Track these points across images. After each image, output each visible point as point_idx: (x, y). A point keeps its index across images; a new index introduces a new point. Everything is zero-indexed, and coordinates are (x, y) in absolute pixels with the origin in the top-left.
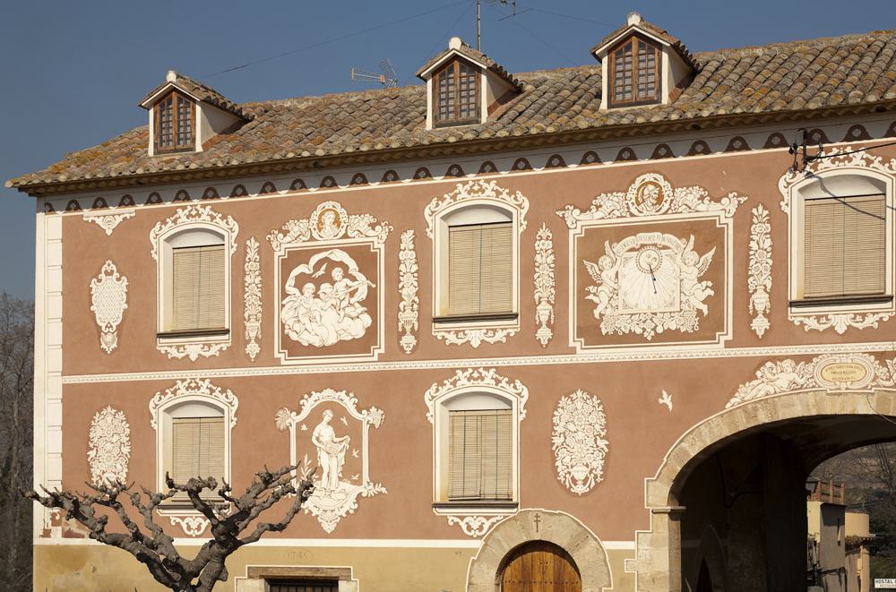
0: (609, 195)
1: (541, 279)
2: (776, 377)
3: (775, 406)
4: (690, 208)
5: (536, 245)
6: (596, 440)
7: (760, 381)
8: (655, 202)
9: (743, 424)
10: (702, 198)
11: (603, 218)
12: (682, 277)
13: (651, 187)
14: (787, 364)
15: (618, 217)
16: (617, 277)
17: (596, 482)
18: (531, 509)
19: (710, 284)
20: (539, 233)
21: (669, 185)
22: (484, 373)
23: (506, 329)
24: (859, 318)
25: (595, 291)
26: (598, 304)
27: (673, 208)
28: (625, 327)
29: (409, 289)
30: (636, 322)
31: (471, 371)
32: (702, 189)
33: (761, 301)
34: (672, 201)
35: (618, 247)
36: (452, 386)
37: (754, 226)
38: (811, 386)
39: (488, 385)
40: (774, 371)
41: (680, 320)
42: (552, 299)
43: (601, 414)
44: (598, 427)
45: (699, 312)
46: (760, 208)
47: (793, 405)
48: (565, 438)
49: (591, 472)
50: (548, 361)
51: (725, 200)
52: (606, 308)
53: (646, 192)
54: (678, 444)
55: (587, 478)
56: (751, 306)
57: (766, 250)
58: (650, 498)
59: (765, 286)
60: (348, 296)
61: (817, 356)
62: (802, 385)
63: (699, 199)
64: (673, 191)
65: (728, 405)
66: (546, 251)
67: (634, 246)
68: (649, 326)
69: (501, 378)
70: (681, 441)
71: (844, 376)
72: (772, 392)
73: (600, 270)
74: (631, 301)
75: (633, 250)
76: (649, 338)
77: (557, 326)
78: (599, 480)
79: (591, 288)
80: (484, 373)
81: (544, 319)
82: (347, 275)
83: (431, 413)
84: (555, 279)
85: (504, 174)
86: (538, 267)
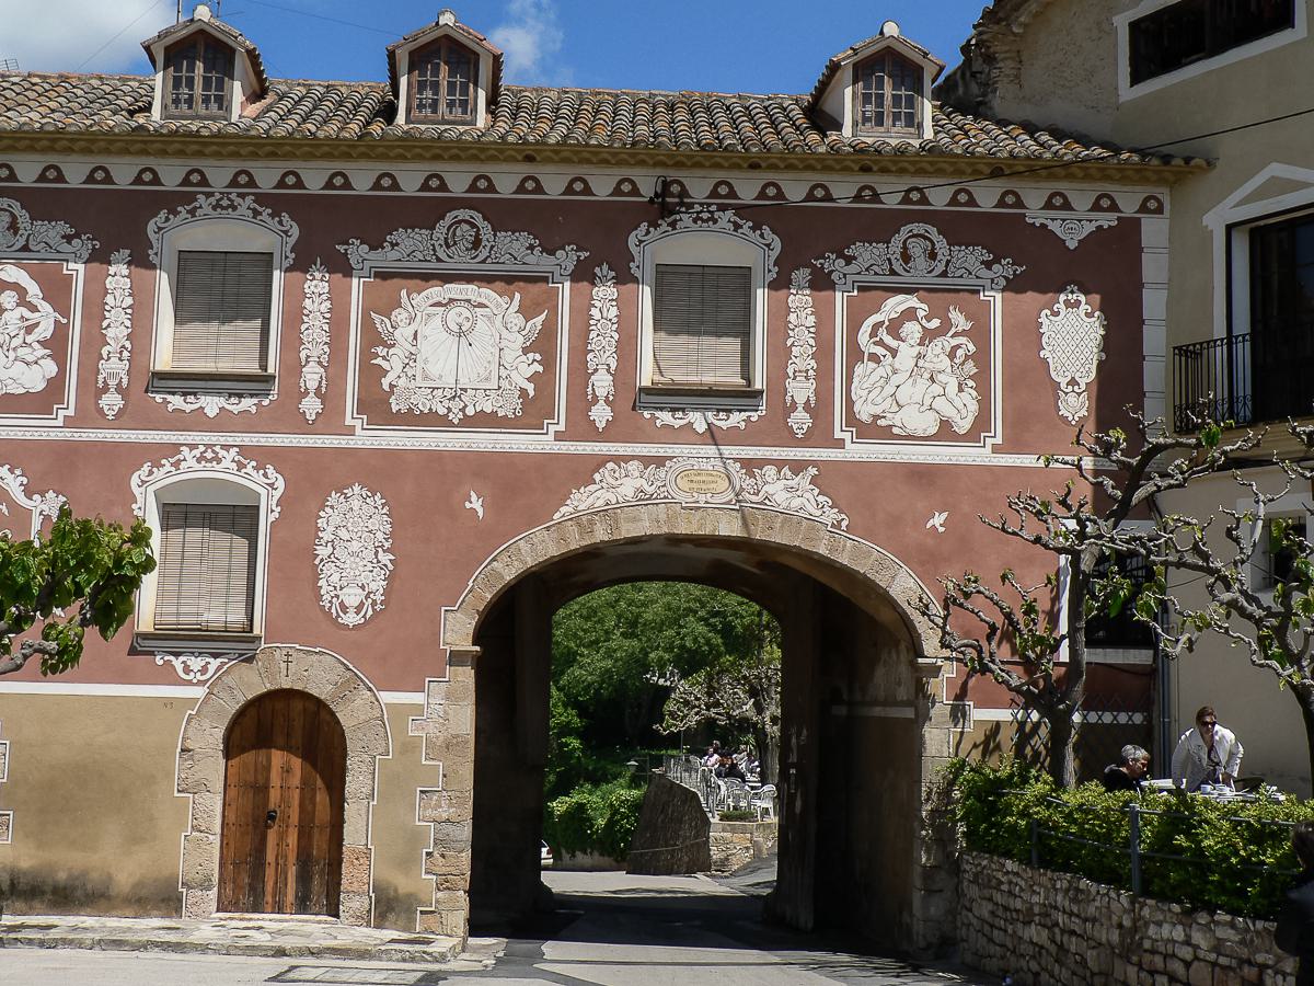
0: (409, 231)
2: (619, 482)
3: (616, 521)
4: (516, 259)
5: (306, 286)
6: (376, 553)
9: (576, 542)
10: (531, 248)
12: (502, 346)
13: (466, 227)
14: (634, 466)
15: (420, 260)
16: (415, 338)
17: (374, 610)
19: (538, 357)
22: (222, 453)
27: (493, 256)
29: (117, 329)
30: (438, 400)
31: (202, 448)
33: (602, 383)
34: (492, 247)
35: (418, 299)
36: (173, 469)
38: (662, 496)
39: (226, 469)
40: (617, 475)
44: (380, 536)
46: (605, 267)
48: (334, 549)
49: (367, 597)
50: (291, 442)
53: (458, 232)
54: (489, 564)
55: (362, 604)
57: (610, 320)
60: (23, 332)
61: (671, 458)
63: (527, 249)
64: (495, 235)
68: (456, 405)
69: (246, 462)
70: (494, 560)
71: (704, 487)
72: (614, 501)
73: (392, 327)
74: (433, 370)
75: (438, 304)
76: (456, 421)
77: (330, 395)
78: (378, 607)
79: (379, 349)
80: (222, 453)
81: (312, 385)
82: (23, 301)
83: (140, 502)
86: (308, 316)
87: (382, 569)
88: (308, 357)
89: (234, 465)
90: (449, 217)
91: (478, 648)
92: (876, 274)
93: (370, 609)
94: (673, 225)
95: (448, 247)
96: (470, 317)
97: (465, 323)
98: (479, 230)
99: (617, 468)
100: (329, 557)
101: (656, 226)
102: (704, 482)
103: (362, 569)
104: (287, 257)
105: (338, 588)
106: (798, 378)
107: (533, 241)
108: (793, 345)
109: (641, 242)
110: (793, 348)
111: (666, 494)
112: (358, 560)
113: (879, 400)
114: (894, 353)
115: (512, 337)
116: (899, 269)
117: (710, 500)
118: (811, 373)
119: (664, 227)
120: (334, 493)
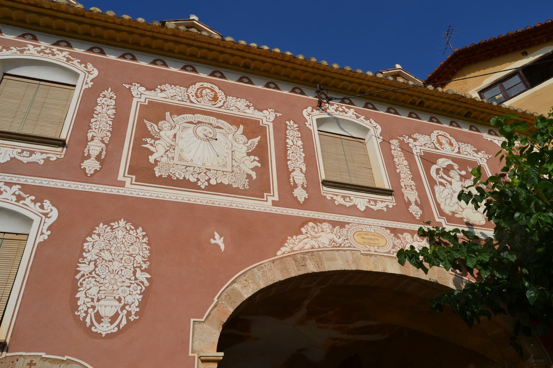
0: (173, 86)
1: (98, 123)
2: (318, 235)
3: (320, 259)
4: (239, 109)
5: (99, 99)
6: (135, 273)
7: (305, 236)
11: (166, 98)
12: (233, 149)
13: (208, 91)
14: (326, 226)
15: (179, 100)
17: (128, 320)
18: (24, 354)
19: (257, 158)
20: (104, 93)
21: (223, 93)
23: (46, 153)
24: (372, 203)
26: (154, 153)
27: (225, 106)
28: (180, 174)
30: (190, 173)
32: (248, 102)
33: (299, 177)
34: (225, 102)
35: (176, 118)
37: (288, 131)
38: (347, 245)
40: (316, 230)
43: (145, 246)
44: (139, 259)
45: (249, 176)
46: (292, 122)
47: (336, 260)
48: (96, 267)
49: (123, 308)
51: (265, 111)
52: (162, 157)
53: (204, 92)
54: (230, 285)
55: (117, 315)
56: (291, 180)
57: (299, 146)
58: (196, 343)
61: (348, 223)
62: (341, 244)
63: (246, 106)
64: (226, 97)
65: (279, 253)
66: (108, 106)
67: (193, 121)
68: (203, 178)
69: (25, 196)
70: (234, 282)
71: (372, 242)
72: (317, 246)
73: (159, 129)
74: (187, 156)
76: (203, 187)
78: (132, 318)
79: (148, 140)
85: (77, 50)
86: (97, 114)
87: (138, 285)
88: (95, 137)
89: (14, 198)
90: (198, 85)
91: (222, 354)
92: (429, 147)
93: (124, 318)
95: (197, 97)
98: (216, 93)
99: (316, 226)
100: (91, 273)
102: (371, 239)
103: (119, 284)
104: (87, 83)
105: (95, 300)
106: (408, 189)
107: (249, 104)
108: (400, 172)
109: (309, 114)
110: (401, 174)
111: (350, 245)
112: (117, 277)
113: (451, 204)
114: (451, 183)
116: (439, 148)
117: (377, 250)
118: (413, 187)
120: (101, 224)
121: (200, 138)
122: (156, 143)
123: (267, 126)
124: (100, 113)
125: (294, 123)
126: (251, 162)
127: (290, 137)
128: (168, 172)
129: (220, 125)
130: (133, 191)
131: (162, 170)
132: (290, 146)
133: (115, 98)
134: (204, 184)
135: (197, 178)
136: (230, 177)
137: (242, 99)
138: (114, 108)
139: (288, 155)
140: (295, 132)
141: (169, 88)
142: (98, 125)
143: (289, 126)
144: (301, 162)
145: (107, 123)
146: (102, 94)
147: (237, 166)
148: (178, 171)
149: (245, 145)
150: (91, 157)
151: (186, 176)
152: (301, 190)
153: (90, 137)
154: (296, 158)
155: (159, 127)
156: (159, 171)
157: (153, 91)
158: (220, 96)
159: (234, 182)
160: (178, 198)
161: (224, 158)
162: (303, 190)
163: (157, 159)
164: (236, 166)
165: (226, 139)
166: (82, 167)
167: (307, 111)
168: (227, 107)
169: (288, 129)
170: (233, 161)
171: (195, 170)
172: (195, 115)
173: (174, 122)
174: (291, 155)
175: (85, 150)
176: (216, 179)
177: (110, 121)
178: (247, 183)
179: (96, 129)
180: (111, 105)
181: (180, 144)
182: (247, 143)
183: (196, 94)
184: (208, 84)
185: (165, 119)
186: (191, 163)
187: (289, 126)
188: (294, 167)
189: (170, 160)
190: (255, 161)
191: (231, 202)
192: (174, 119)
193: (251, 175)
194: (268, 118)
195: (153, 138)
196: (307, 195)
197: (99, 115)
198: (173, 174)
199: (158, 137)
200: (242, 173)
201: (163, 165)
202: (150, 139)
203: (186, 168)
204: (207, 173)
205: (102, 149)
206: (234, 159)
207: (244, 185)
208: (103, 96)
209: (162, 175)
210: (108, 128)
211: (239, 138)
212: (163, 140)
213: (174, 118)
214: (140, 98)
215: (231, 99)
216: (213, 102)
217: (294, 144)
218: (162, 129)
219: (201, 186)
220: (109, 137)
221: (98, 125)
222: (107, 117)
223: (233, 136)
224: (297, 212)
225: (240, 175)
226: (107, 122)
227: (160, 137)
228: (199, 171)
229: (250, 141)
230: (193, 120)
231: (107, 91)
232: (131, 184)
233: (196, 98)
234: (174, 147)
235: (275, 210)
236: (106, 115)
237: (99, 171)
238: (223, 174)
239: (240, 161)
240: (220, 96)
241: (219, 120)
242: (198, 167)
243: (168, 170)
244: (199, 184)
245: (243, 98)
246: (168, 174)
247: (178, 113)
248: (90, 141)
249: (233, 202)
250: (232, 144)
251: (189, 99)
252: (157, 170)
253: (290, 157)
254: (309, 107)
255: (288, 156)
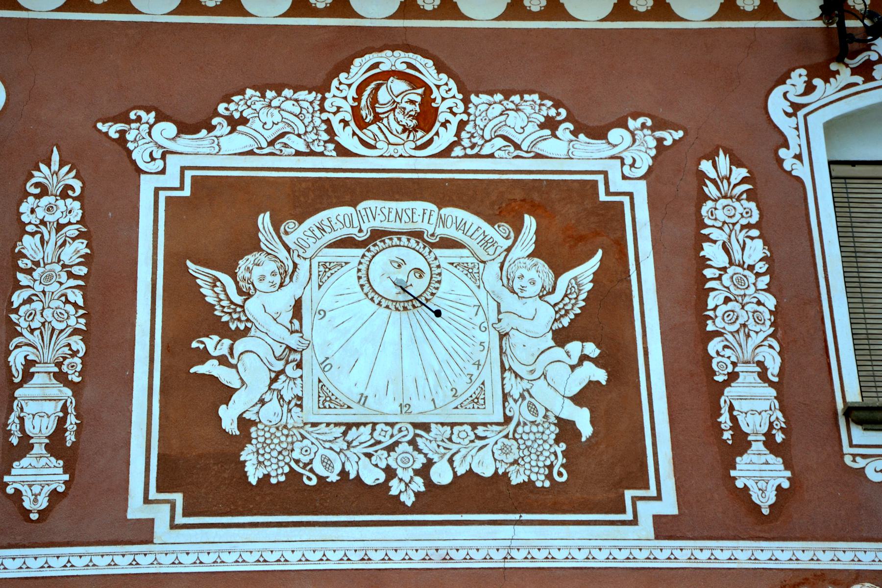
0: (270, 94)
1: (37, 306)
4: (517, 147)
5: (25, 208)
8: (412, 123)
11: (251, 153)
12: (504, 326)
13: (399, 86)
15: (298, 153)
19: (592, 350)
20: (38, 177)
21: (452, 84)
25: (223, 349)
26: (235, 390)
27: (466, 143)
28: (327, 463)
30: (360, 450)
32: (549, 103)
34: (462, 125)
37: (709, 204)
41: (505, 450)
42: (74, 369)
46: (723, 161)
51: (615, 135)
52: (262, 402)
53: (383, 96)
56: (725, 419)
57: (751, 268)
59: (760, 364)
63: (542, 126)
64: (466, 101)
66: (60, 227)
73: (240, 292)
76: (408, 499)
79: (210, 343)
84: (88, 311)
86: (29, 272)
88: (33, 363)
90: (360, 68)
94: (866, 71)
95: (362, 124)
96: (426, 269)
97: (413, 279)
98: (428, 90)
101: (828, 76)
109: (796, 107)
115: (528, 308)
119: (845, 76)
121: (384, 303)
122: (236, 354)
123: (626, 200)
124: (37, 264)
125: (731, 163)
126: (573, 368)
127: (715, 234)
128: (287, 460)
129: (451, 232)
130: (182, 552)
131: (267, 456)
132: (718, 273)
133: (78, 192)
134: (414, 487)
135: (383, 466)
136: (499, 445)
137: (526, 97)
138: (81, 235)
139: (711, 313)
140: (737, 204)
141: (258, 106)
142: (38, 316)
143: (713, 181)
144: (762, 336)
145: (67, 301)
146: (34, 180)
147: (522, 396)
148: (322, 451)
149: (547, 298)
150: (32, 447)
151: (348, 467)
152: (763, 459)
153: (20, 368)
154: (741, 321)
155: (241, 284)
156: (259, 463)
157: (204, 132)
158: (443, 99)
159: (516, 462)
160: (329, 555)
161: (473, 370)
162: (771, 458)
163: (247, 416)
164: (516, 396)
165: (473, 286)
166: (10, 490)
167: (785, 95)
168: (473, 147)
169: (707, 198)
170: (507, 374)
171: (376, 434)
172: (361, 206)
173: (288, 249)
174: (720, 312)
175: (10, 421)
176: (451, 461)
177: (77, 291)
178: (561, 460)
179: (32, 331)
180: (69, 223)
181: (316, 341)
182: (554, 289)
183: (355, 111)
184: (397, 53)
185: (256, 247)
186: (357, 409)
187: (713, 181)
188: (734, 364)
189: (289, 411)
190: (587, 364)
191: (508, 543)
192: (289, 240)
193: (572, 423)
194: (628, 161)
195: (224, 331)
196: (788, 474)
197: (36, 275)
198: (306, 465)
199: (242, 327)
200: (539, 419)
201: (268, 435)
202: (216, 338)
203: (345, 434)
204: (418, 439)
205: (64, 409)
206: (510, 369)
207: (551, 467)
208: (37, 191)
209: (267, 476)
210: (72, 321)
211: (522, 277)
212: (259, 334)
213: (287, 233)
214: (163, 172)
215: (485, 107)
216: (420, 134)
217: (731, 263)
218: (252, 291)
219: (403, 498)
220: (81, 354)
221: (38, 316)
222: (64, 276)
223: (501, 268)
224: (748, 554)
225: (534, 429)
226: (65, 295)
227: (249, 325)
228: (392, 436)
229: (565, 279)
230: (356, 231)
231: (49, 166)
232: (173, 526)
233: (358, 131)
234: (298, 357)
235: (666, 553)
236: (58, 268)
237: (64, 494)
238: (472, 437)
239: (532, 372)
240: (443, 99)
241: (447, 211)
242: (387, 424)
243: (285, 453)
244: (394, 492)
245: (531, 92)
246: (287, 469)
247: (298, 210)
248: (20, 385)
249: (515, 543)
250: (499, 305)
251: (331, 140)
252: (251, 457)
253: (718, 321)
254: (794, 75)
255: (709, 317)
